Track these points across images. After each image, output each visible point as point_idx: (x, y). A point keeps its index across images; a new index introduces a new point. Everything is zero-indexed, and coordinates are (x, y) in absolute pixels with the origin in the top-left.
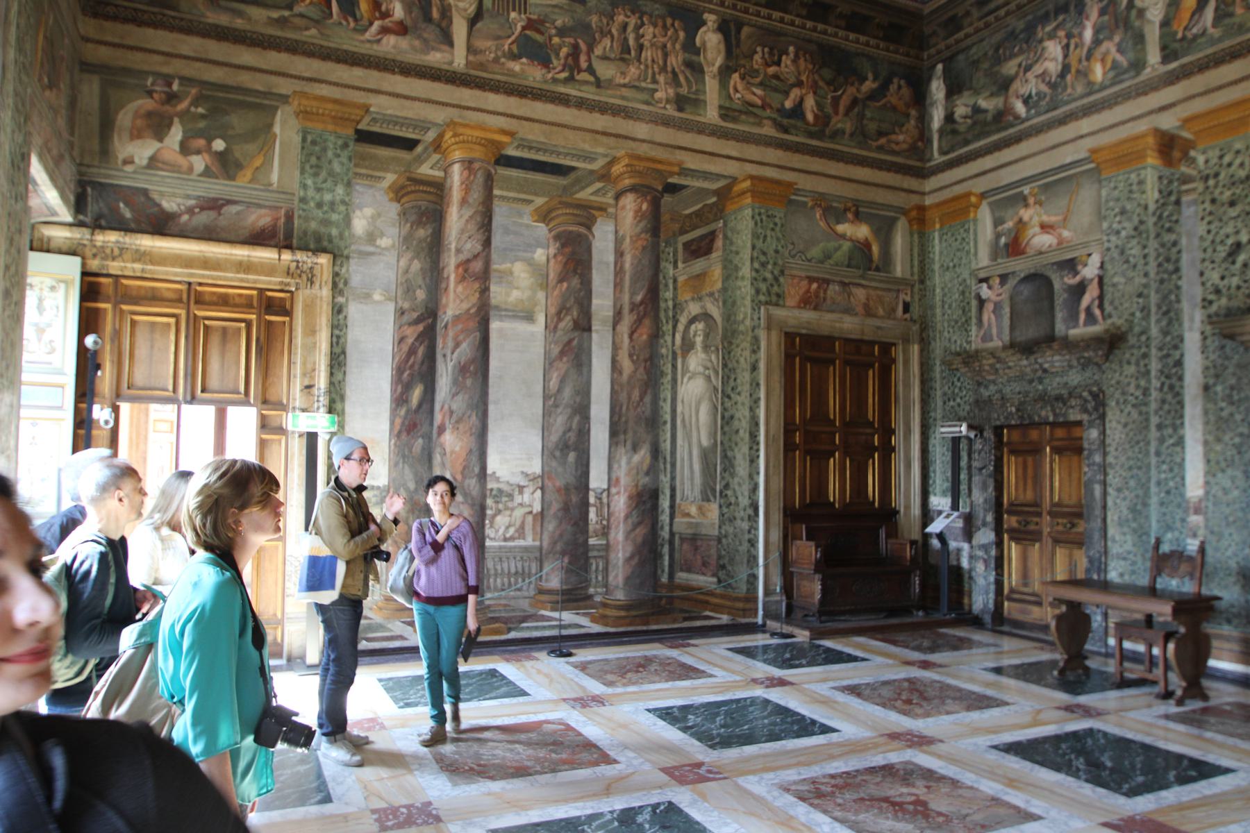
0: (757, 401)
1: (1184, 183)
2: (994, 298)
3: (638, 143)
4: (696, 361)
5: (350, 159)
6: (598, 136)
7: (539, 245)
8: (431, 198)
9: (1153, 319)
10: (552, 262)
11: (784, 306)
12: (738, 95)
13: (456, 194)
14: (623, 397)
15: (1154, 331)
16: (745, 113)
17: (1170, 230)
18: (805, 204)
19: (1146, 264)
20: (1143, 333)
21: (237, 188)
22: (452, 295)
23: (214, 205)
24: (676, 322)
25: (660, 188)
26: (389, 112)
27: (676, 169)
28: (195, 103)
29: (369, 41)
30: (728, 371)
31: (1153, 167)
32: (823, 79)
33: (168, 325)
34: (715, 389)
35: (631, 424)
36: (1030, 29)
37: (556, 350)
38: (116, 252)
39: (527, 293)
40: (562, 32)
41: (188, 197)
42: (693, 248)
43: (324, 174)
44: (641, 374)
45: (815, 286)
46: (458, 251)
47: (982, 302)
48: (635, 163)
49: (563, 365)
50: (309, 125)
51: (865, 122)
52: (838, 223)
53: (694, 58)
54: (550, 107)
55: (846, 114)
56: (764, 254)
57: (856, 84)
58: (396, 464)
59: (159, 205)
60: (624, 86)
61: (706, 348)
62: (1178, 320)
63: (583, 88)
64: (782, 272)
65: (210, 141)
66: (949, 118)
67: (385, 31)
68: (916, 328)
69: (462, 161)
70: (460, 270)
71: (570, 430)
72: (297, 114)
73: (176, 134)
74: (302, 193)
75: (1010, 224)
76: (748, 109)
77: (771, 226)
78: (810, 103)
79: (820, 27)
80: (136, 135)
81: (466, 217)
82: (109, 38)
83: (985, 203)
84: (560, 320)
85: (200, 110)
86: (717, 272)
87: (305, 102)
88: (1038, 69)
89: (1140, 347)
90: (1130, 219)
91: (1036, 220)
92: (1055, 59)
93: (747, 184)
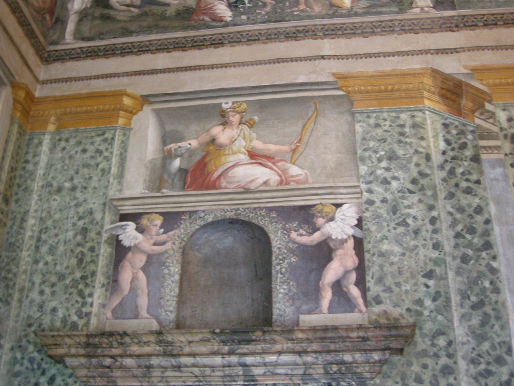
1: (482, 137)
2: (147, 246)
9: (456, 314)
15: (460, 332)
17: (468, 191)
19: (435, 231)
20: (439, 333)
31: (433, 111)
47: (120, 251)
62: (498, 318)
83: (147, 109)
89: (436, 356)
90: (404, 168)
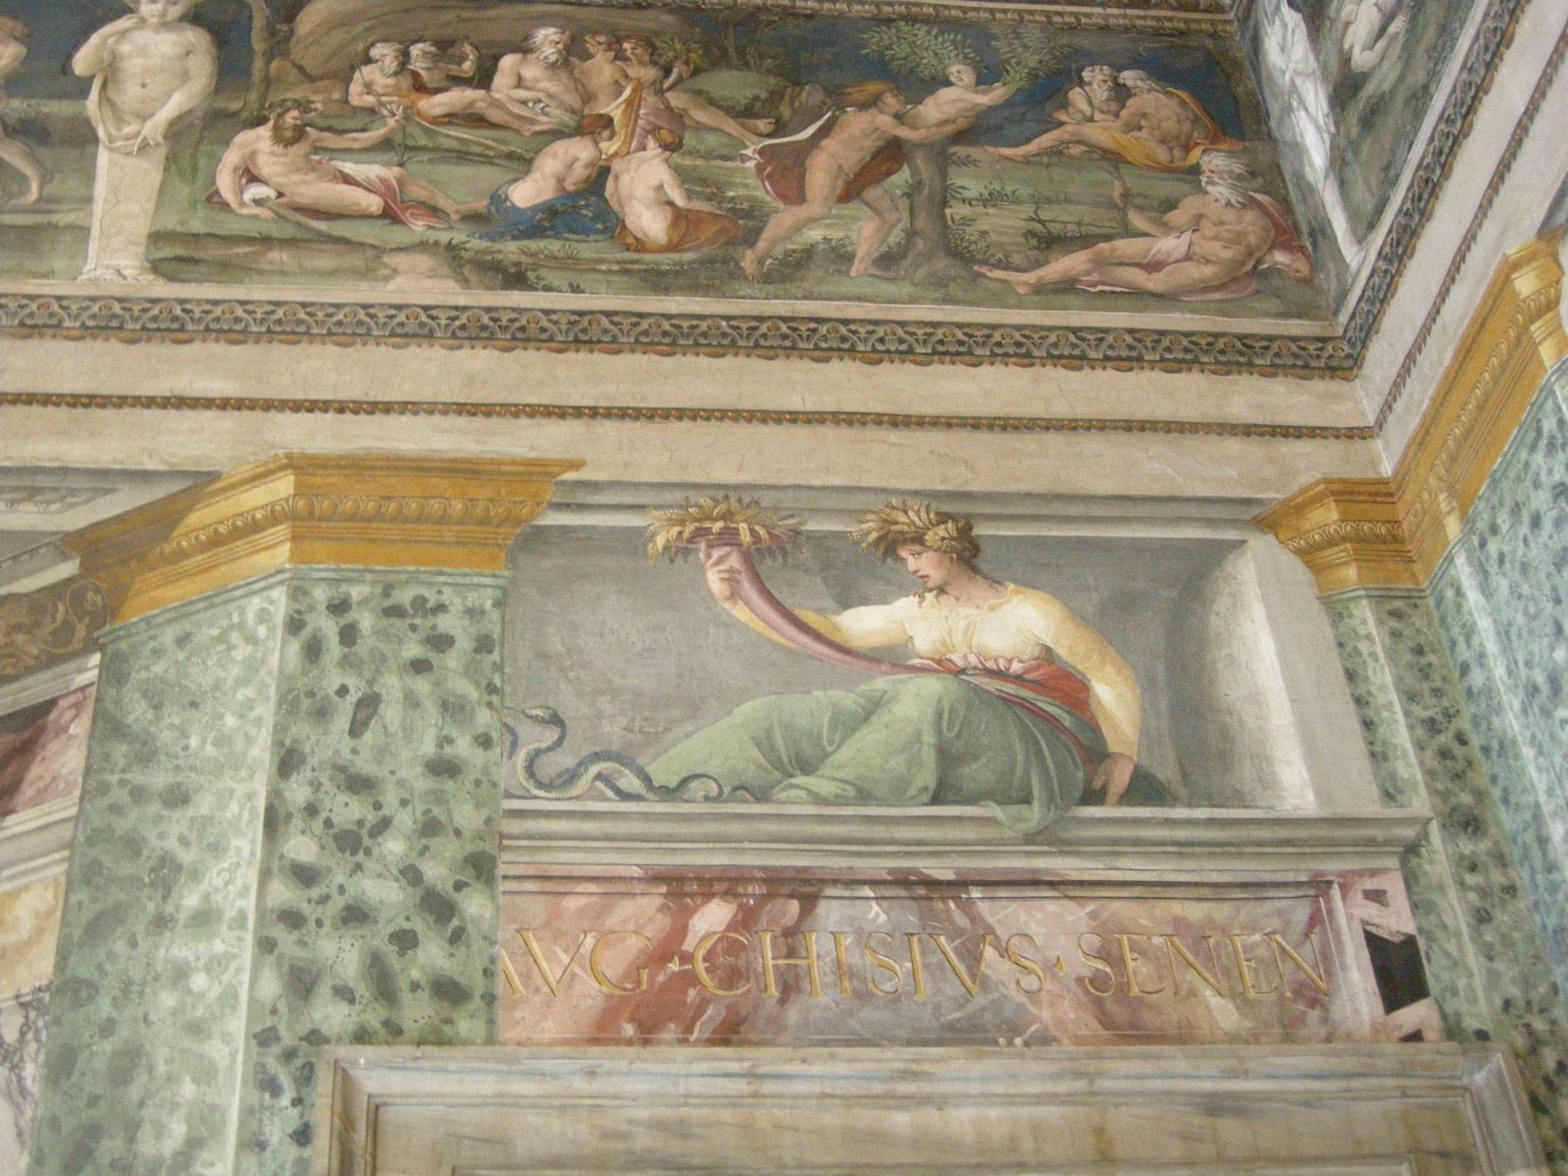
16: (290, 243)
18: (634, 541)
45: (713, 917)
51: (955, 211)
52: (846, 603)
55: (851, 191)
56: (358, 784)
57: (891, 101)
64: (481, 867)
76: (309, 229)
77: (413, 649)
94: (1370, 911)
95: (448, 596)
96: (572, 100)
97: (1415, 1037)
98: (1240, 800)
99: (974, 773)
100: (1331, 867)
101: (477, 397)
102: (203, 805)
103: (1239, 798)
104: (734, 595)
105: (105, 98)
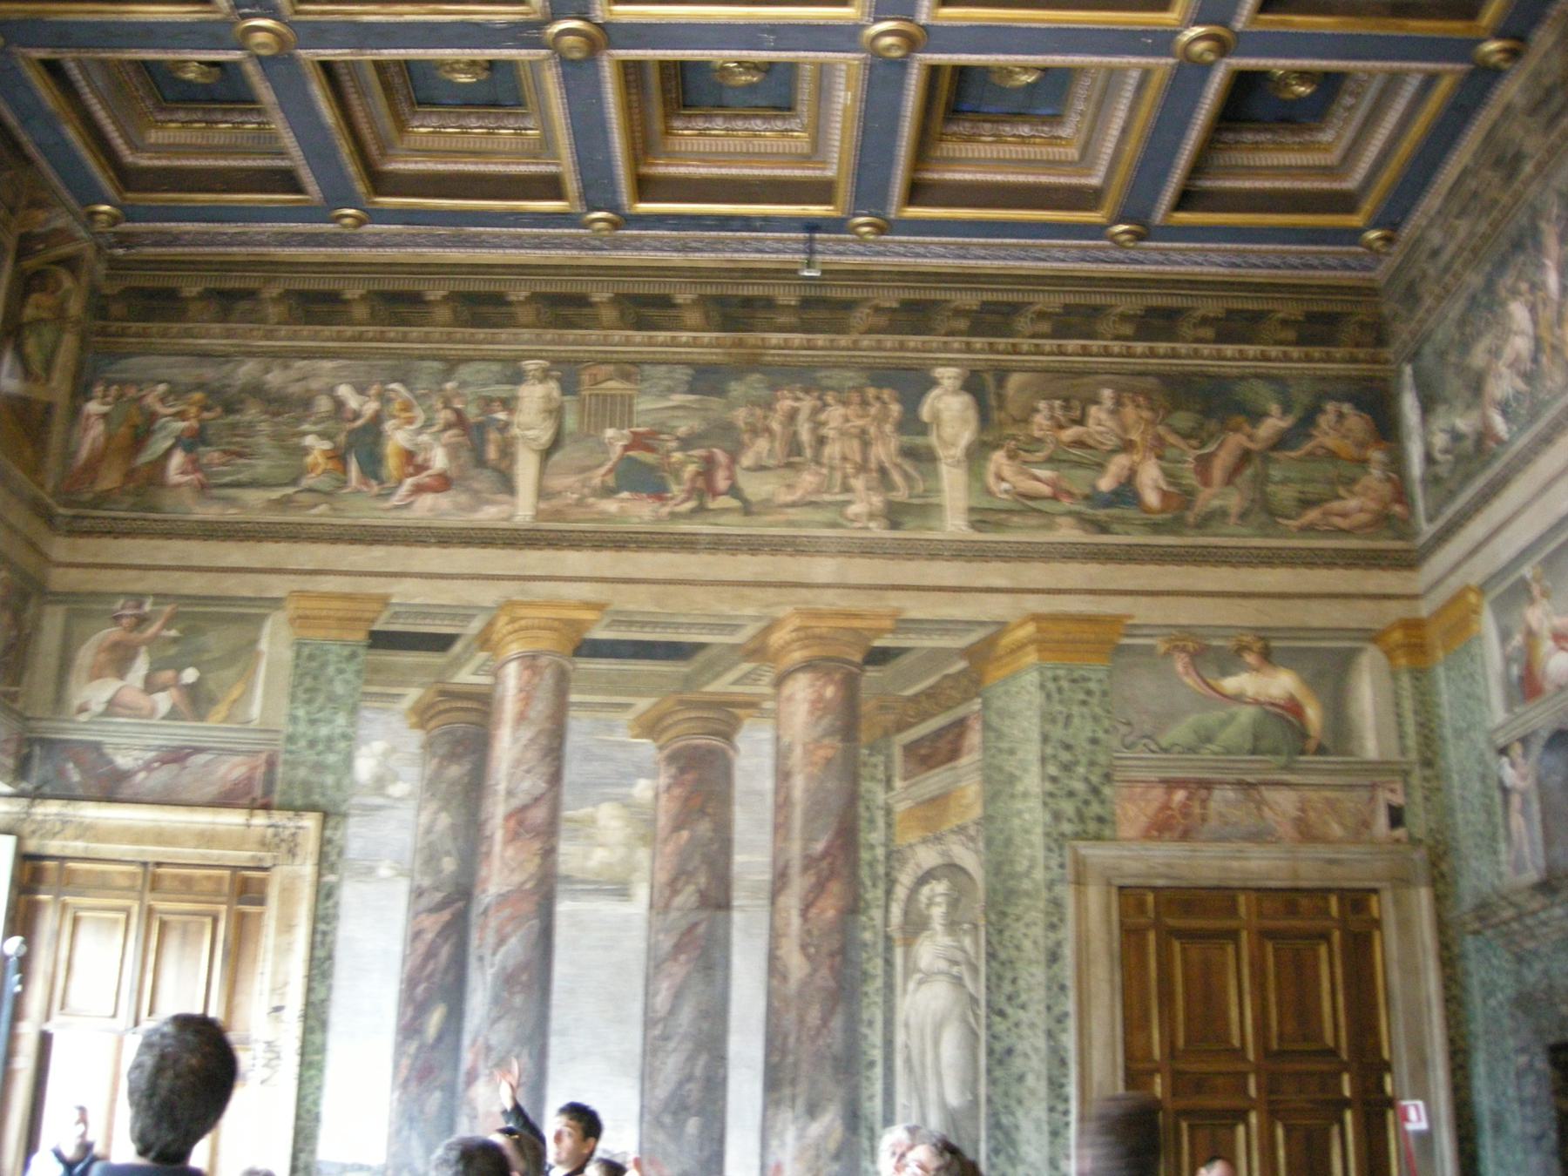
0: (1061, 1019)
2: (1520, 784)
3: (816, 591)
4: (931, 950)
5: (358, 673)
6: (746, 591)
7: (641, 772)
8: (473, 717)
10: (664, 799)
11: (1114, 839)
12: (1005, 486)
13: (509, 706)
14: (790, 1018)
18: (1150, 650)
21: (210, 729)
22: (496, 862)
23: (176, 756)
24: (891, 882)
25: (858, 658)
26: (417, 601)
27: (887, 623)
28: (167, 625)
29: (397, 508)
30: (999, 963)
32: (1176, 432)
33: (116, 921)
34: (974, 1001)
35: (805, 1067)
36: (1490, 287)
37: (667, 943)
38: (58, 827)
39: (620, 852)
40: (686, 443)
41: (147, 748)
42: (923, 751)
43: (321, 699)
44: (824, 977)
45: (1180, 795)
46: (510, 793)
47: (1506, 791)
48: (813, 623)
49: (678, 970)
50: (309, 633)
51: (1271, 488)
52: (1225, 673)
53: (919, 440)
54: (665, 558)
55: (1229, 481)
56: (1068, 747)
57: (1247, 428)
58: (399, 1131)
59: (110, 762)
60: (793, 505)
61: (952, 926)
63: (723, 519)
65: (180, 669)
66: (1429, 459)
67: (419, 489)
68: (1419, 856)
69: (521, 658)
70: (512, 823)
71: (690, 1078)
72: (292, 621)
73: (141, 667)
74: (290, 729)
75: (1518, 640)
76: (1025, 504)
77: (1082, 696)
78: (1150, 479)
79: (1162, 347)
80: (96, 674)
81: (524, 741)
82: (80, 559)
84: (675, 892)
85: (173, 633)
86: (972, 789)
87: (304, 603)
88: (1508, 353)
91: (1546, 633)
92: (1522, 333)
93: (1030, 629)
94: (1389, 796)
95: (1092, 676)
96: (1118, 431)
97: (1398, 841)
98: (1351, 754)
99: (1265, 744)
100: (1382, 779)
101: (1094, 587)
102: (1020, 755)
103: (1351, 754)
104: (1187, 674)
105: (939, 437)
